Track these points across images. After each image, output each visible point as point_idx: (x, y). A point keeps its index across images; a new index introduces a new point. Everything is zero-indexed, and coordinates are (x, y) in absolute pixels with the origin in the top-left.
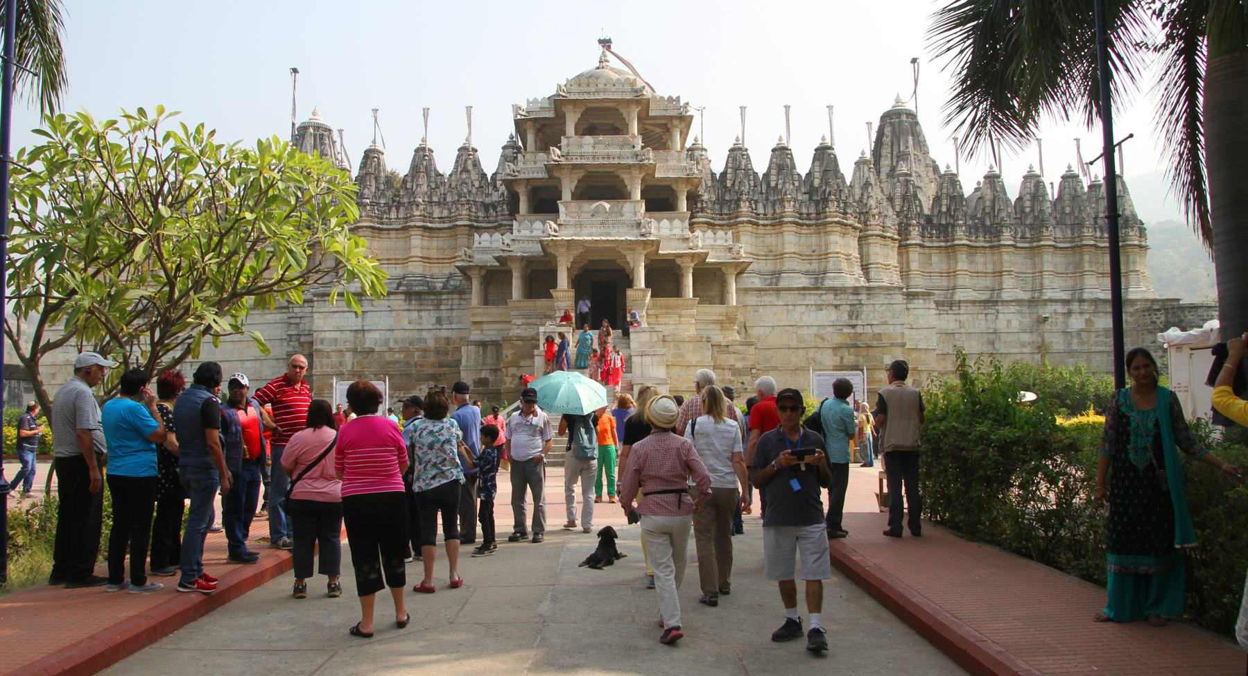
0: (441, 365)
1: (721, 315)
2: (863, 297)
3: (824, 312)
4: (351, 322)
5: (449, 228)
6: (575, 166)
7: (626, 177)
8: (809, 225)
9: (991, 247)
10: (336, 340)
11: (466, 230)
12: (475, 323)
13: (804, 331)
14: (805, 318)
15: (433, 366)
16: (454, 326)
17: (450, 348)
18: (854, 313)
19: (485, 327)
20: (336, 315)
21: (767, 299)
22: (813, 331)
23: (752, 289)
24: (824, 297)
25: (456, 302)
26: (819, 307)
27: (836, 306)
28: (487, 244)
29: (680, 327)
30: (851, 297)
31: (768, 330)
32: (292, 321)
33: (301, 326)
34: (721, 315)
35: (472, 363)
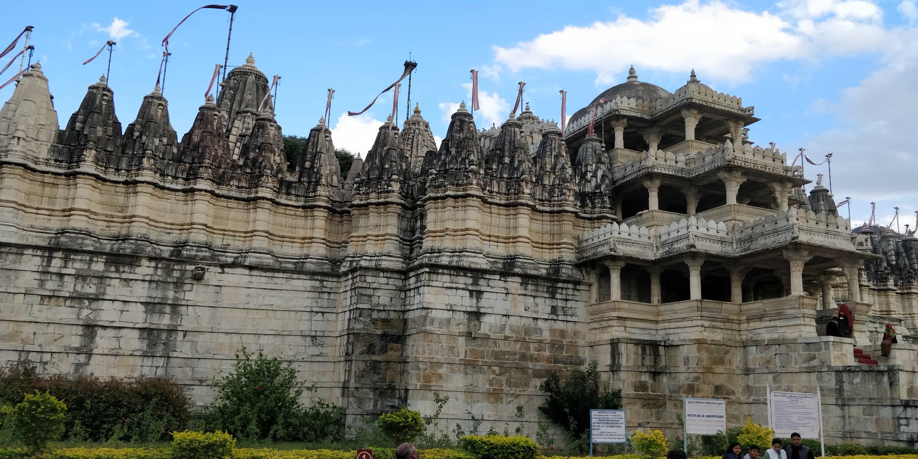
0: (556, 361)
4: (466, 302)
5: (551, 212)
6: (746, 171)
7: (777, 188)
9: (879, 290)
10: (448, 321)
11: (572, 217)
12: (619, 318)
15: (548, 360)
16: (569, 318)
17: (565, 342)
19: (628, 323)
20: (449, 292)
25: (570, 292)
28: (624, 235)
32: (364, 292)
33: (375, 300)
35: (631, 363)
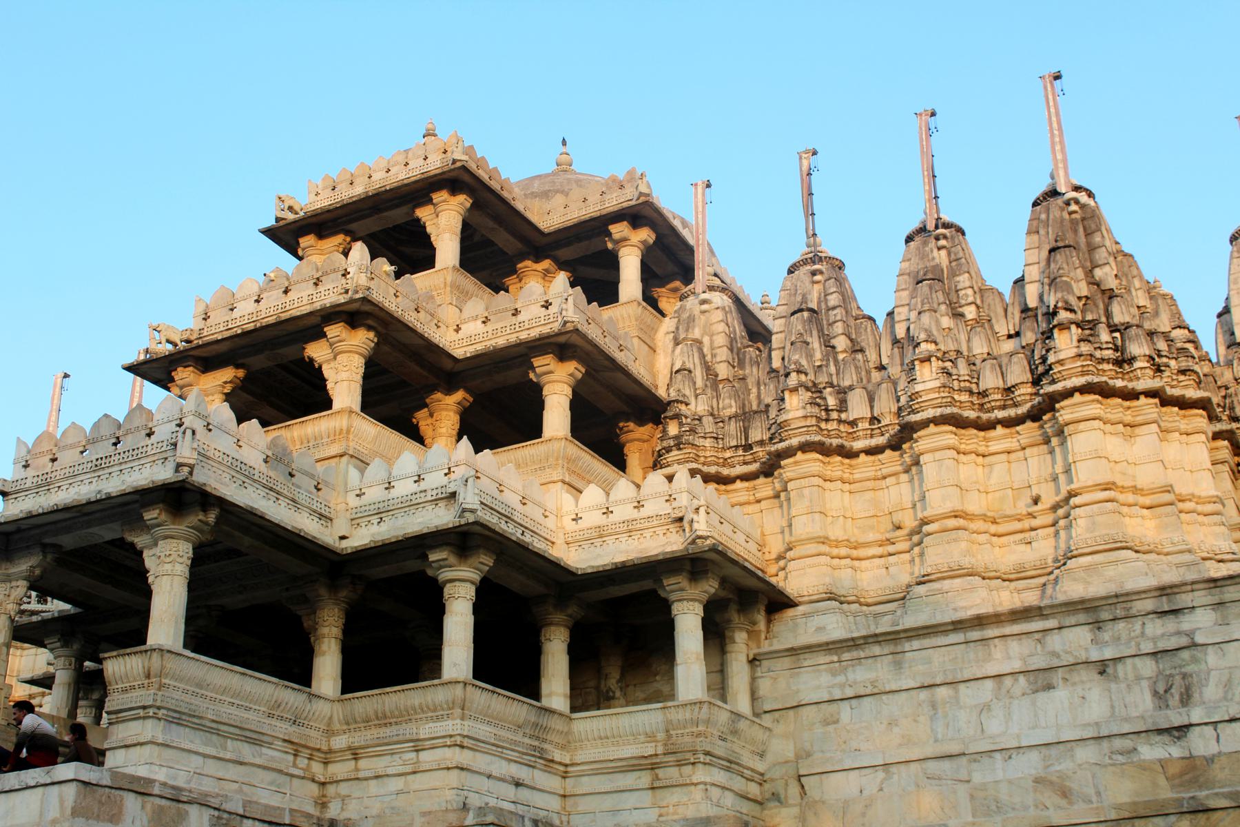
1: (651, 737)
2: (1202, 622)
3: (1061, 695)
8: (1009, 423)
13: (998, 770)
14: (994, 725)
18: (1176, 687)
21: (861, 675)
22: (1029, 765)
23: (809, 649)
24: (1056, 642)
26: (1042, 679)
27: (1103, 667)
29: (417, 782)
30: (1156, 627)
31: (872, 781)
34: (651, 737)
